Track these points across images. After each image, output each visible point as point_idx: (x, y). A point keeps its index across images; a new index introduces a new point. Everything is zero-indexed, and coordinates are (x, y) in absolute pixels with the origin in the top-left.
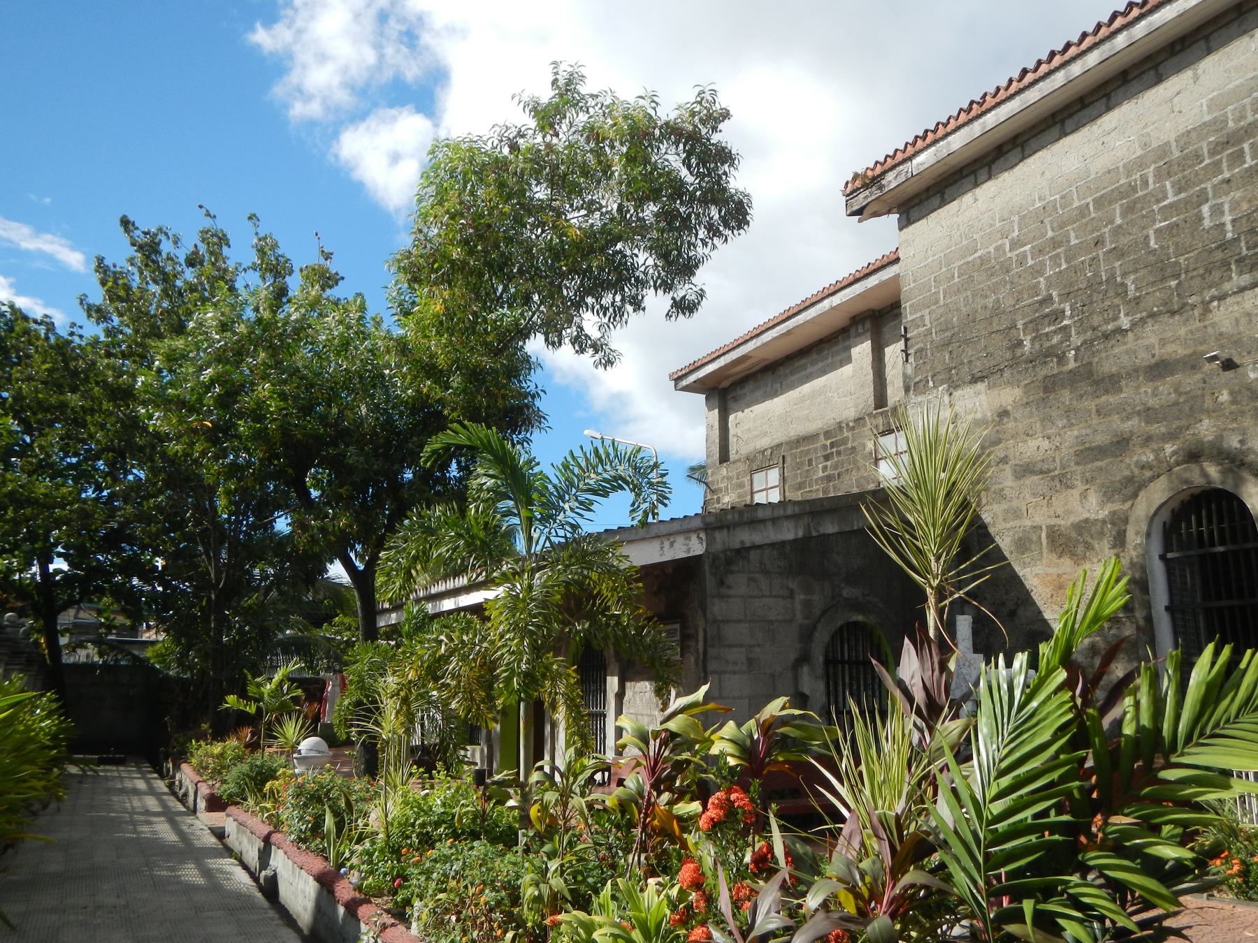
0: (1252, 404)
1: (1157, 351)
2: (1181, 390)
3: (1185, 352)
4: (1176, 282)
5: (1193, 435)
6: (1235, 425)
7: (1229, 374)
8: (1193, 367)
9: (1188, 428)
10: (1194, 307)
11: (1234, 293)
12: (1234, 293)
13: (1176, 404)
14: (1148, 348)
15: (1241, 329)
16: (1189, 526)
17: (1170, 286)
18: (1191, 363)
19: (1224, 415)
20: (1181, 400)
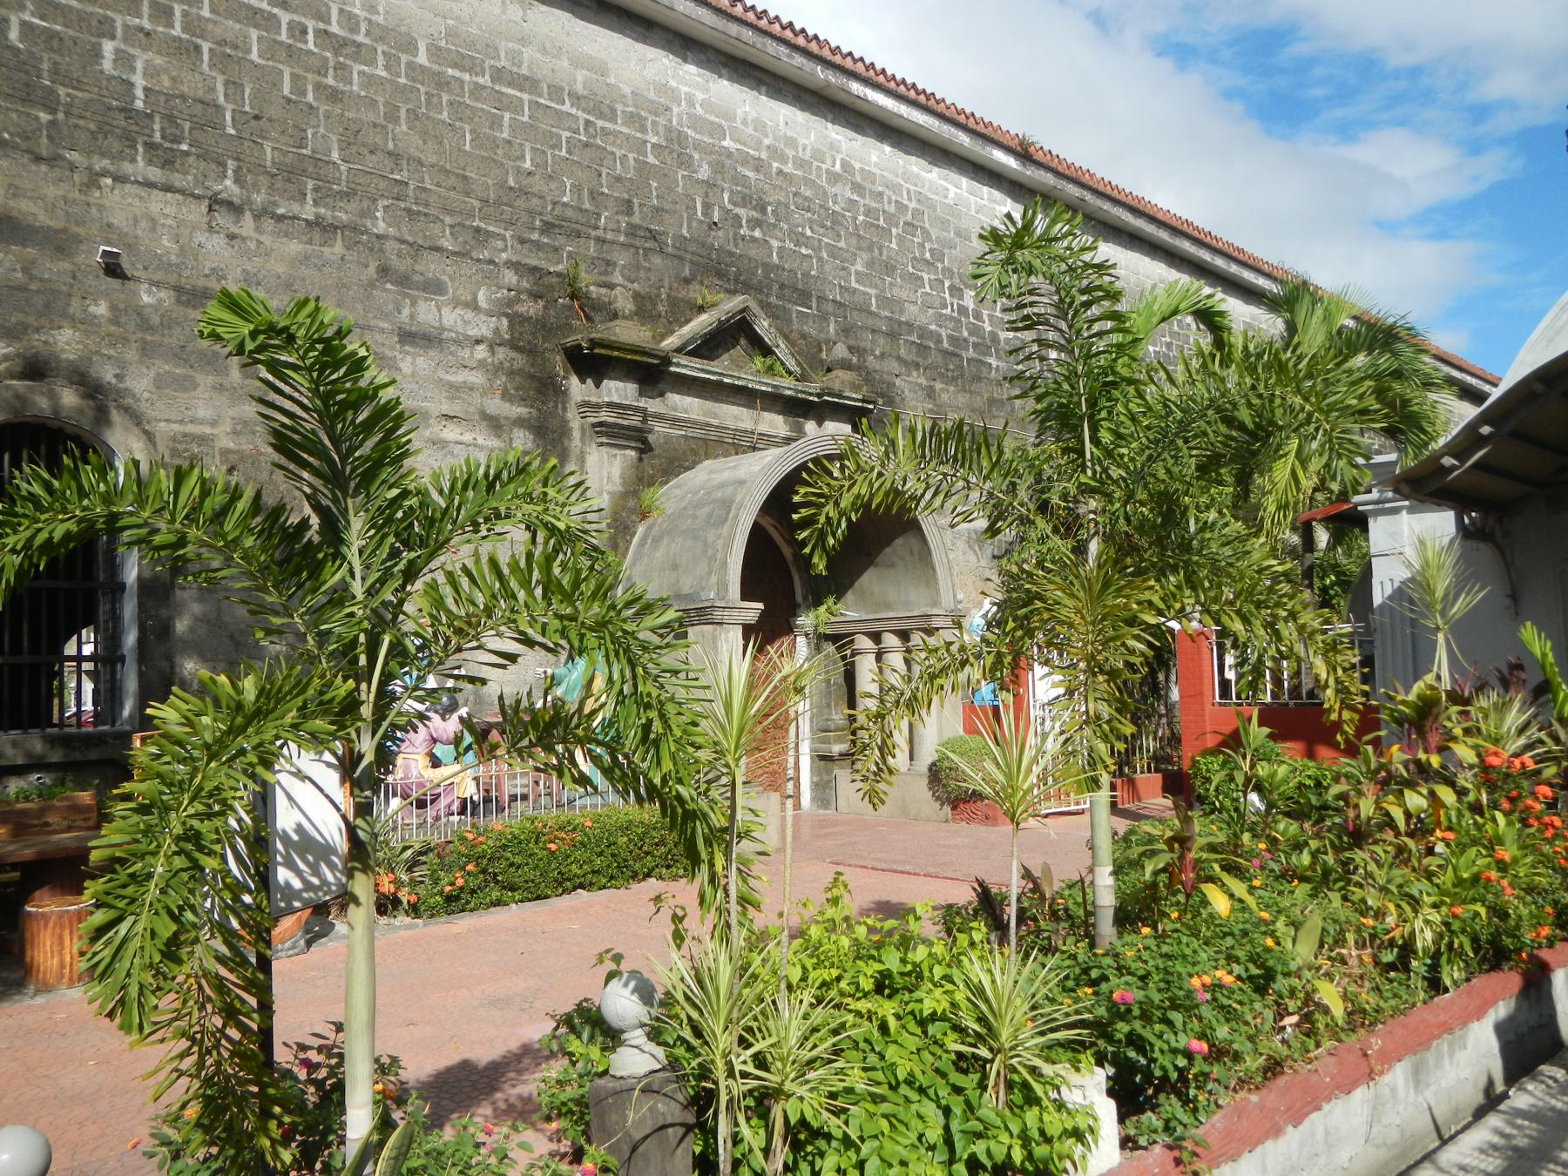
0: (139, 335)
2: (34, 272)
3: (52, 223)
4: (49, 117)
5: (45, 342)
6: (112, 352)
7: (113, 283)
9: (38, 330)
10: (73, 167)
11: (137, 182)
12: (137, 182)
13: (22, 289)
17: (37, 119)
18: (61, 243)
20: (33, 287)
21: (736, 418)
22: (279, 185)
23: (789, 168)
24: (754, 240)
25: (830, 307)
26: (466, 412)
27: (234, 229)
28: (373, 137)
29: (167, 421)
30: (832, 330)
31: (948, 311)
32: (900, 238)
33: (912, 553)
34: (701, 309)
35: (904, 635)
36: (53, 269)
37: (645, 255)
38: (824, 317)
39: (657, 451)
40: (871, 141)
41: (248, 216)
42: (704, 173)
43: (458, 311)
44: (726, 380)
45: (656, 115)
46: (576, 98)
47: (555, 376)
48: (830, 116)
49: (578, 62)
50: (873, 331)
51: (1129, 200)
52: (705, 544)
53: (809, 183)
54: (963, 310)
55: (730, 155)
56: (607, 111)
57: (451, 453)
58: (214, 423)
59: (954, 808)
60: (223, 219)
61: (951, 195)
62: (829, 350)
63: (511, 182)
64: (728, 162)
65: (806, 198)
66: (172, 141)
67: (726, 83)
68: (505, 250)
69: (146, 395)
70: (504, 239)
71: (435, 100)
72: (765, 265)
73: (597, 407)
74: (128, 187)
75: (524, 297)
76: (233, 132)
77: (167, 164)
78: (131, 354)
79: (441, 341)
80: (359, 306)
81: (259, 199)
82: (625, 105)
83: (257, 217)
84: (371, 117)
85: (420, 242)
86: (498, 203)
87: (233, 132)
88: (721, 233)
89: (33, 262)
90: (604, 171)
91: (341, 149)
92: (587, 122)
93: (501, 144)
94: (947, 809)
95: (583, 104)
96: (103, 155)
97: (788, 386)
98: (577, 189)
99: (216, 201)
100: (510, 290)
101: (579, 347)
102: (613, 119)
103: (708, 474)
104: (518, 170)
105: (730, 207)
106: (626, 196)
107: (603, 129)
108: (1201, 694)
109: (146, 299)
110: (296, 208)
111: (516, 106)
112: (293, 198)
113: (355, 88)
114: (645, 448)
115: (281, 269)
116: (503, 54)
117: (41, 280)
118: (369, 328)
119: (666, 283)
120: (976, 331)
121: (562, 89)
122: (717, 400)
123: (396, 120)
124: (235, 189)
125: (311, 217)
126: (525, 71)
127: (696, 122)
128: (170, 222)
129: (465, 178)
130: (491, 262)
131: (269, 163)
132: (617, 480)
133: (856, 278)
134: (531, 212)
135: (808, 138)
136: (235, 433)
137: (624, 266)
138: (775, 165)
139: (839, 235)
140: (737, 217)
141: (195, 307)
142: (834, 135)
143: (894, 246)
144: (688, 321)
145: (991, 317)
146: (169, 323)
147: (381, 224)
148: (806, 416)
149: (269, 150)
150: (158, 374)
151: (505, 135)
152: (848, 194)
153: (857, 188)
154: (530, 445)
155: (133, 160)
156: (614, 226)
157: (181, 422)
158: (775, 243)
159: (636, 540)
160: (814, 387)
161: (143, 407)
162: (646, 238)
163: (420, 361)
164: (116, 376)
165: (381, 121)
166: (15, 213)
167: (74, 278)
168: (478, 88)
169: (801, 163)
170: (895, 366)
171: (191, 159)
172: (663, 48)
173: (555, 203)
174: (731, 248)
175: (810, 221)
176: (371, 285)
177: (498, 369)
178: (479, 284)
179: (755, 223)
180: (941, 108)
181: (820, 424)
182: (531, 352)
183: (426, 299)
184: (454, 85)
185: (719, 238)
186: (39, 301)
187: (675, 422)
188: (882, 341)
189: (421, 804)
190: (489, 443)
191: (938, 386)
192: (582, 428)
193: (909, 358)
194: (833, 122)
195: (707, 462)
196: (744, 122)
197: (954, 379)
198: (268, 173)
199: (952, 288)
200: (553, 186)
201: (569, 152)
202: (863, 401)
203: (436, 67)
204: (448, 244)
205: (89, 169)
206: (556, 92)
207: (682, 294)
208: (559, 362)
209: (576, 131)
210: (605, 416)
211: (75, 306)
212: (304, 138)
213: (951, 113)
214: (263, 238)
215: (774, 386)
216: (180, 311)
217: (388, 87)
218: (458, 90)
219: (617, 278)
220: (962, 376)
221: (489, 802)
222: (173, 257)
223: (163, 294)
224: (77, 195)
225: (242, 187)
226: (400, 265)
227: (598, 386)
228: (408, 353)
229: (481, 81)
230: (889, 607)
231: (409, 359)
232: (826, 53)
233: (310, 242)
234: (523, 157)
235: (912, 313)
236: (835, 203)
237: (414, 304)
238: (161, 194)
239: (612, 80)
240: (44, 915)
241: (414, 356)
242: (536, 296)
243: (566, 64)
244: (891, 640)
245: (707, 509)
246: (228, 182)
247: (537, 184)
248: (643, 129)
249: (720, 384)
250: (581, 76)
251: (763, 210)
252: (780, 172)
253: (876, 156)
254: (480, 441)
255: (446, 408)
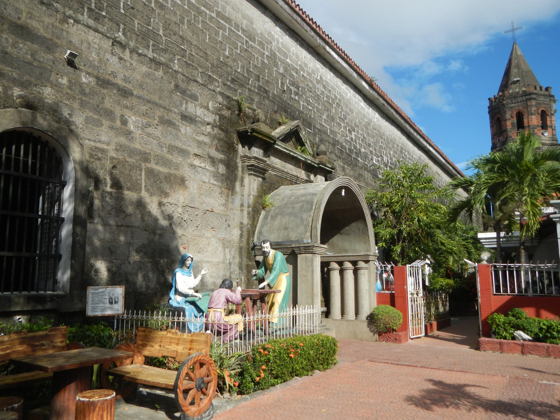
0: (80, 96)
1: (23, 18)
2: (37, 57)
3: (46, 35)
6: (68, 102)
7: (70, 69)
8: (48, 48)
9: (36, 85)
10: (57, 11)
12: (83, 24)
14: (17, 10)
15: (83, 48)
16: (9, 152)
19: (62, 92)
20: (35, 64)
21: (291, 170)
22: (140, 40)
23: (305, 75)
24: (296, 100)
25: (317, 130)
26: (203, 154)
27: (122, 55)
28: (174, 28)
29: (89, 140)
30: (317, 140)
31: (348, 139)
32: (336, 110)
33: (359, 229)
34: (280, 124)
35: (354, 263)
36: (45, 57)
37: (263, 99)
38: (315, 135)
39: (267, 180)
40: (328, 70)
41: (127, 51)
42: (281, 70)
43: (202, 109)
44: (292, 154)
45: (268, 44)
46: (243, 31)
47: (233, 143)
48: (317, 58)
49: (245, 17)
50: (329, 143)
51: (395, 107)
52: (302, 219)
53: (311, 82)
54: (352, 139)
55: (289, 66)
56: (253, 38)
57: (197, 171)
58: (108, 144)
59: (380, 335)
60: (117, 50)
61: (348, 96)
62: (317, 148)
63: (222, 60)
64: (288, 68)
65: (310, 87)
66: (100, 10)
67: (288, 37)
68: (218, 87)
69: (81, 126)
70: (218, 82)
71: (197, 19)
72: (299, 110)
73: (250, 158)
74: (80, 25)
75: (224, 108)
76: (122, 11)
77: (96, 19)
78: (76, 105)
79: (196, 121)
80: (167, 100)
81: (132, 44)
82: (258, 38)
83: (131, 52)
84: (174, 19)
85: (190, 77)
86: (217, 66)
87: (122, 11)
88: (286, 95)
89: (36, 52)
90: (252, 62)
91: (163, 30)
92: (247, 41)
93: (218, 42)
94: (376, 336)
95: (245, 33)
96: (70, 8)
97: (309, 159)
98: (243, 67)
99: (115, 41)
100: (220, 104)
101: (247, 132)
102: (254, 42)
103: (285, 191)
104: (224, 54)
105: (289, 85)
106: (258, 74)
107: (251, 45)
108: (490, 289)
109: (84, 80)
110: (146, 52)
111: (223, 28)
112: (144, 47)
113: (169, 5)
114: (264, 179)
115: (139, 77)
116: (220, 6)
117: (39, 61)
118: (171, 111)
119: (269, 112)
120: (355, 147)
121: (239, 26)
122: (286, 162)
123: (183, 23)
124: (123, 38)
125: (151, 57)
126: (227, 15)
127: (279, 50)
128: (96, 46)
129: (206, 54)
130: (214, 91)
131: (136, 29)
132: (256, 190)
133: (322, 121)
134: (228, 74)
135: (311, 65)
136: (117, 150)
137: (257, 102)
138: (302, 72)
139: (319, 104)
140: (291, 90)
141: (104, 88)
142: (318, 65)
143: (334, 111)
144: (276, 128)
145: (359, 143)
146: (93, 93)
147: (177, 66)
148: (311, 172)
149: (136, 24)
150: (87, 117)
151: (220, 39)
152: (322, 89)
153: (324, 87)
154: (224, 172)
155: (83, 14)
156: (253, 85)
157: (95, 141)
158: (302, 103)
159: (262, 216)
160: (317, 161)
161: (79, 131)
162: (263, 92)
163: (188, 128)
164: (69, 114)
165: (178, 22)
166: (29, 26)
167: (54, 63)
168: (211, 18)
169: (309, 74)
170: (333, 157)
171: (106, 20)
172: (270, 18)
173: (236, 71)
174: (289, 101)
175: (312, 96)
176: (172, 92)
177: (214, 137)
178: (210, 99)
179: (296, 94)
180: (350, 62)
181: (315, 176)
182: (226, 131)
183: (191, 102)
184: (204, 14)
185: (285, 97)
186: (37, 71)
187: (274, 168)
188: (331, 147)
189: (219, 333)
190: (210, 169)
191: (346, 167)
192: (242, 167)
193: (338, 154)
194: (317, 60)
195: (282, 187)
196: (293, 54)
197: (350, 164)
198: (136, 34)
199: (349, 130)
200: (235, 64)
201: (240, 51)
202: (331, 168)
203: (197, 5)
204: (199, 80)
205: (64, 13)
206: (237, 26)
207: (274, 117)
208: (235, 137)
209: (243, 44)
210: (252, 162)
211: (53, 78)
212: (150, 22)
213: (353, 64)
214: (133, 62)
215: (305, 158)
216: (97, 89)
217: (181, 9)
218: (204, 17)
219: (255, 107)
220: (352, 163)
221: (246, 334)
222: (96, 63)
223: (91, 79)
224: (58, 24)
225: (126, 37)
226: (183, 85)
227: (249, 149)
228: (184, 124)
229: (213, 15)
230: (346, 251)
231: (184, 126)
232: (321, 33)
233: (150, 68)
234: (226, 50)
235: (339, 137)
236: (318, 91)
237: (187, 103)
238: (93, 32)
239: (254, 27)
240: (93, 403)
241: (186, 126)
242: (229, 109)
243: (240, 16)
244: (348, 265)
245: (299, 205)
246: (120, 34)
247: (230, 63)
248: (264, 49)
249: (289, 155)
250: (245, 22)
251: (298, 89)
252: (303, 76)
253: (329, 76)
254: (207, 167)
255: (196, 151)
